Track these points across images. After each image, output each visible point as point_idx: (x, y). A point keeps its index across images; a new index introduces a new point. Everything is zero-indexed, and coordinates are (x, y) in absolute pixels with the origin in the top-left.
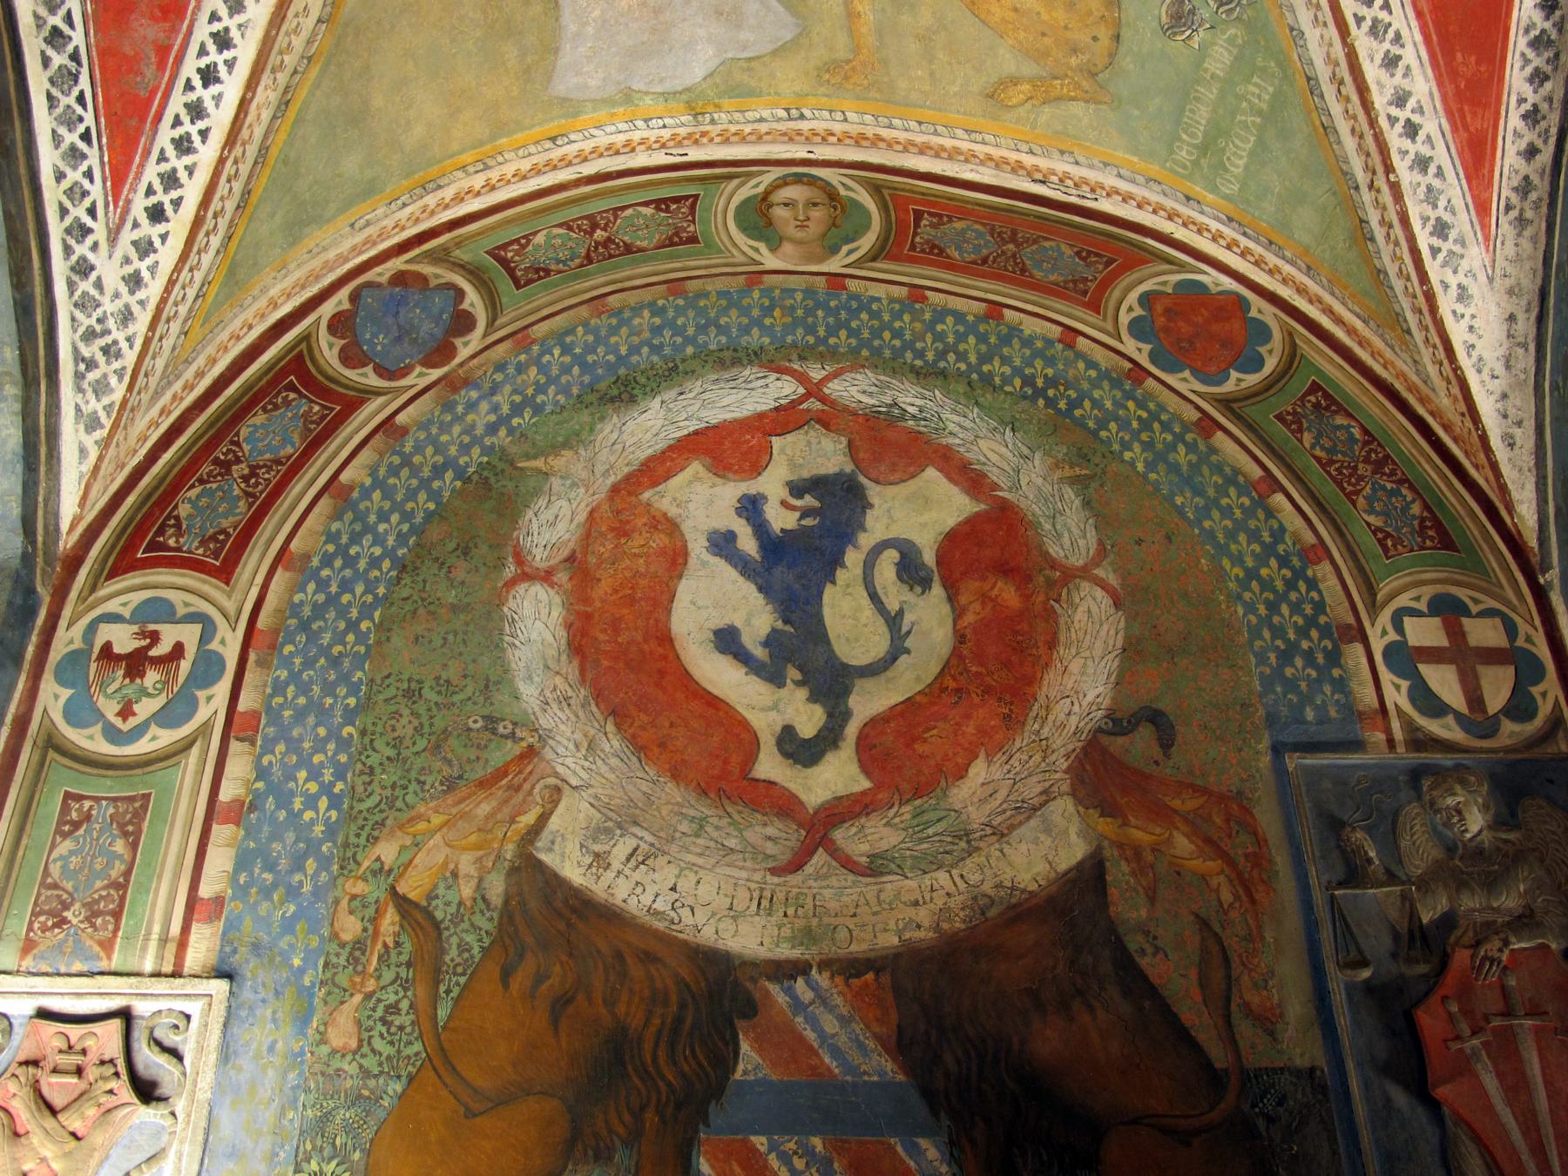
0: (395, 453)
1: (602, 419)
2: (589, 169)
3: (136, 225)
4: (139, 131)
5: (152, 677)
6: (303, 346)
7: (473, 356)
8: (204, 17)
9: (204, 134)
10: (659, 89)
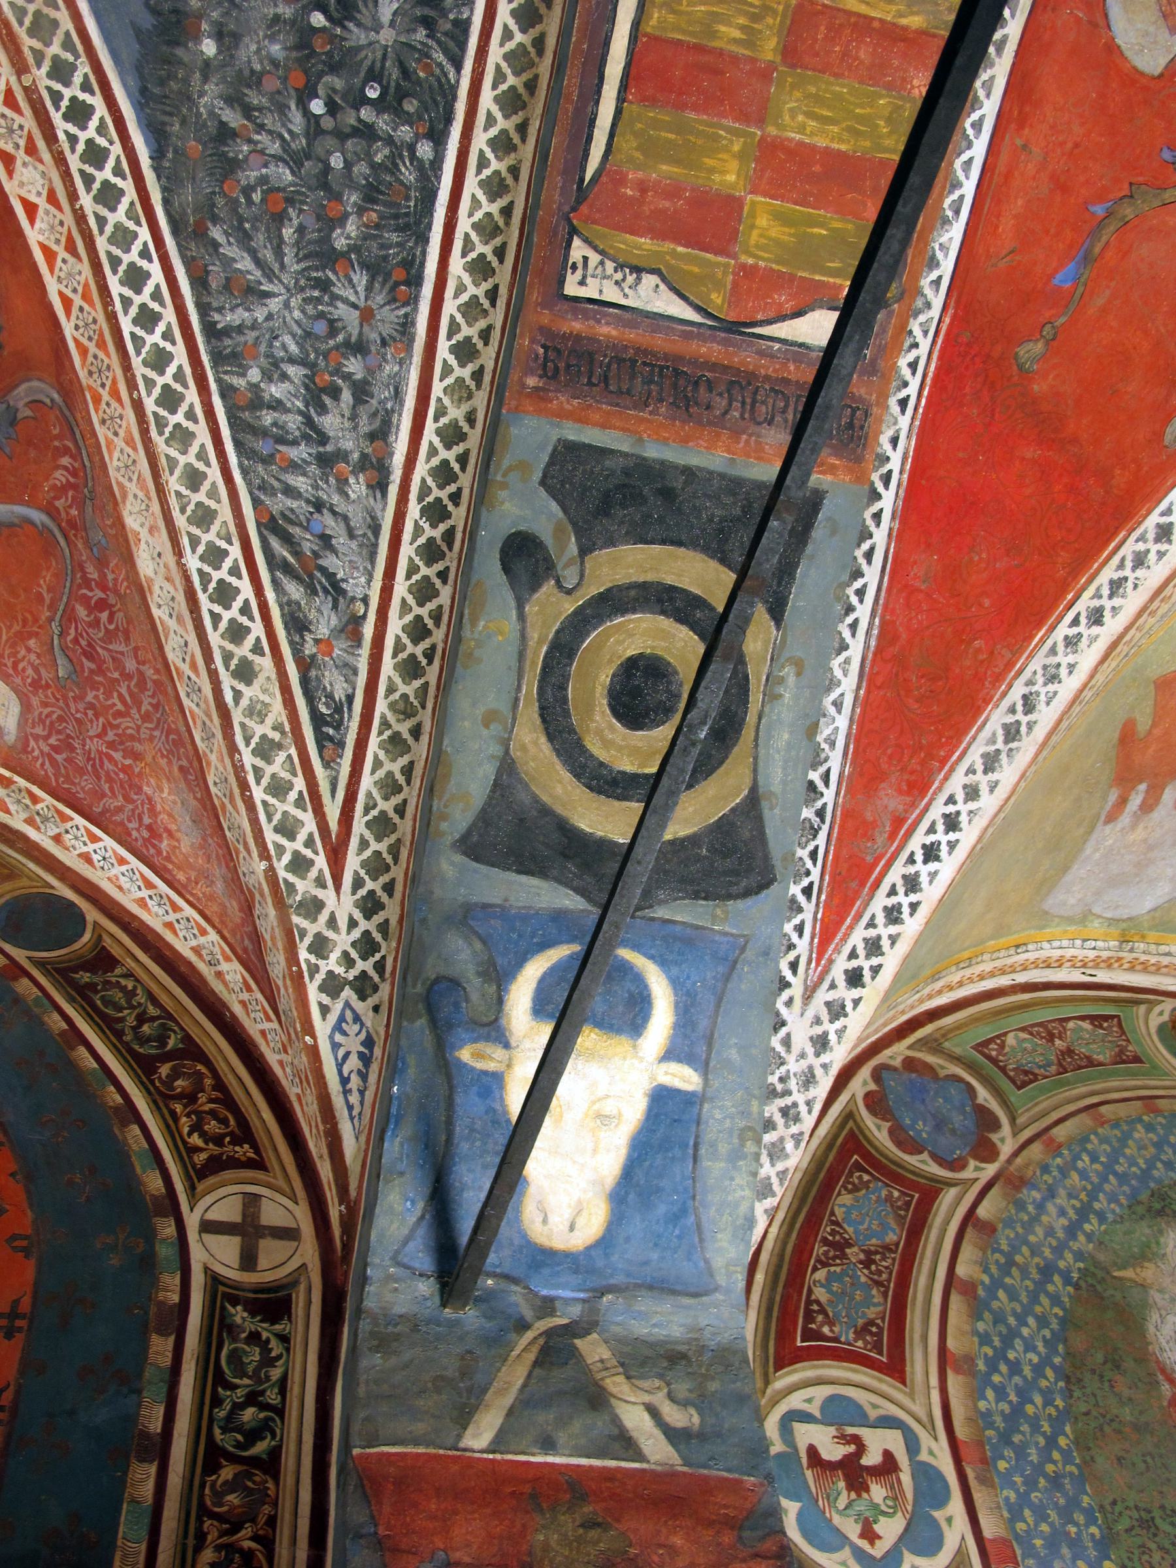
0: (994, 1251)
1: (1161, 1232)
2: (1021, 978)
3: (833, 986)
4: (857, 894)
5: (878, 1492)
6: (851, 1124)
7: (1016, 1154)
8: (943, 797)
9: (914, 907)
10: (1109, 915)
